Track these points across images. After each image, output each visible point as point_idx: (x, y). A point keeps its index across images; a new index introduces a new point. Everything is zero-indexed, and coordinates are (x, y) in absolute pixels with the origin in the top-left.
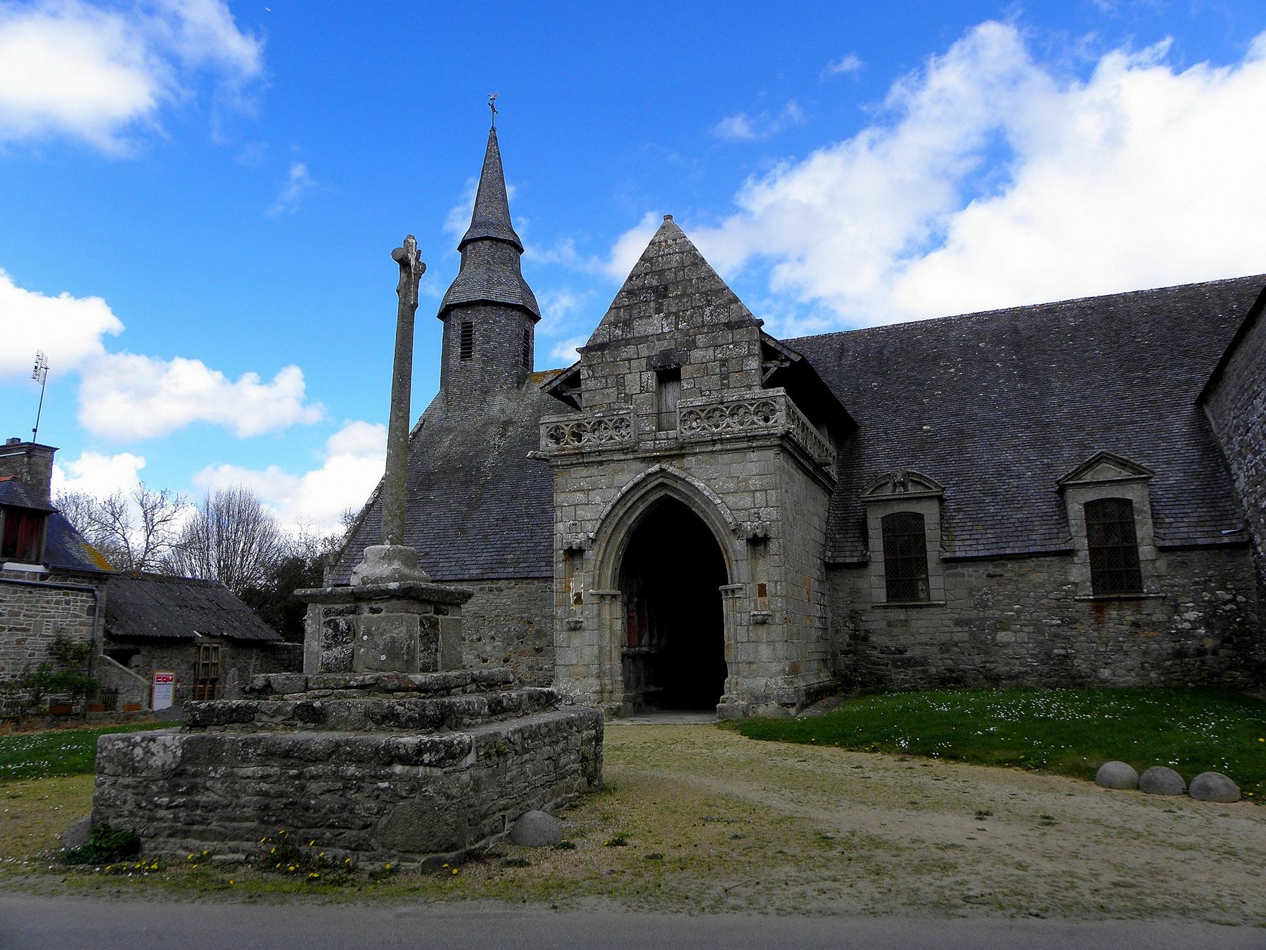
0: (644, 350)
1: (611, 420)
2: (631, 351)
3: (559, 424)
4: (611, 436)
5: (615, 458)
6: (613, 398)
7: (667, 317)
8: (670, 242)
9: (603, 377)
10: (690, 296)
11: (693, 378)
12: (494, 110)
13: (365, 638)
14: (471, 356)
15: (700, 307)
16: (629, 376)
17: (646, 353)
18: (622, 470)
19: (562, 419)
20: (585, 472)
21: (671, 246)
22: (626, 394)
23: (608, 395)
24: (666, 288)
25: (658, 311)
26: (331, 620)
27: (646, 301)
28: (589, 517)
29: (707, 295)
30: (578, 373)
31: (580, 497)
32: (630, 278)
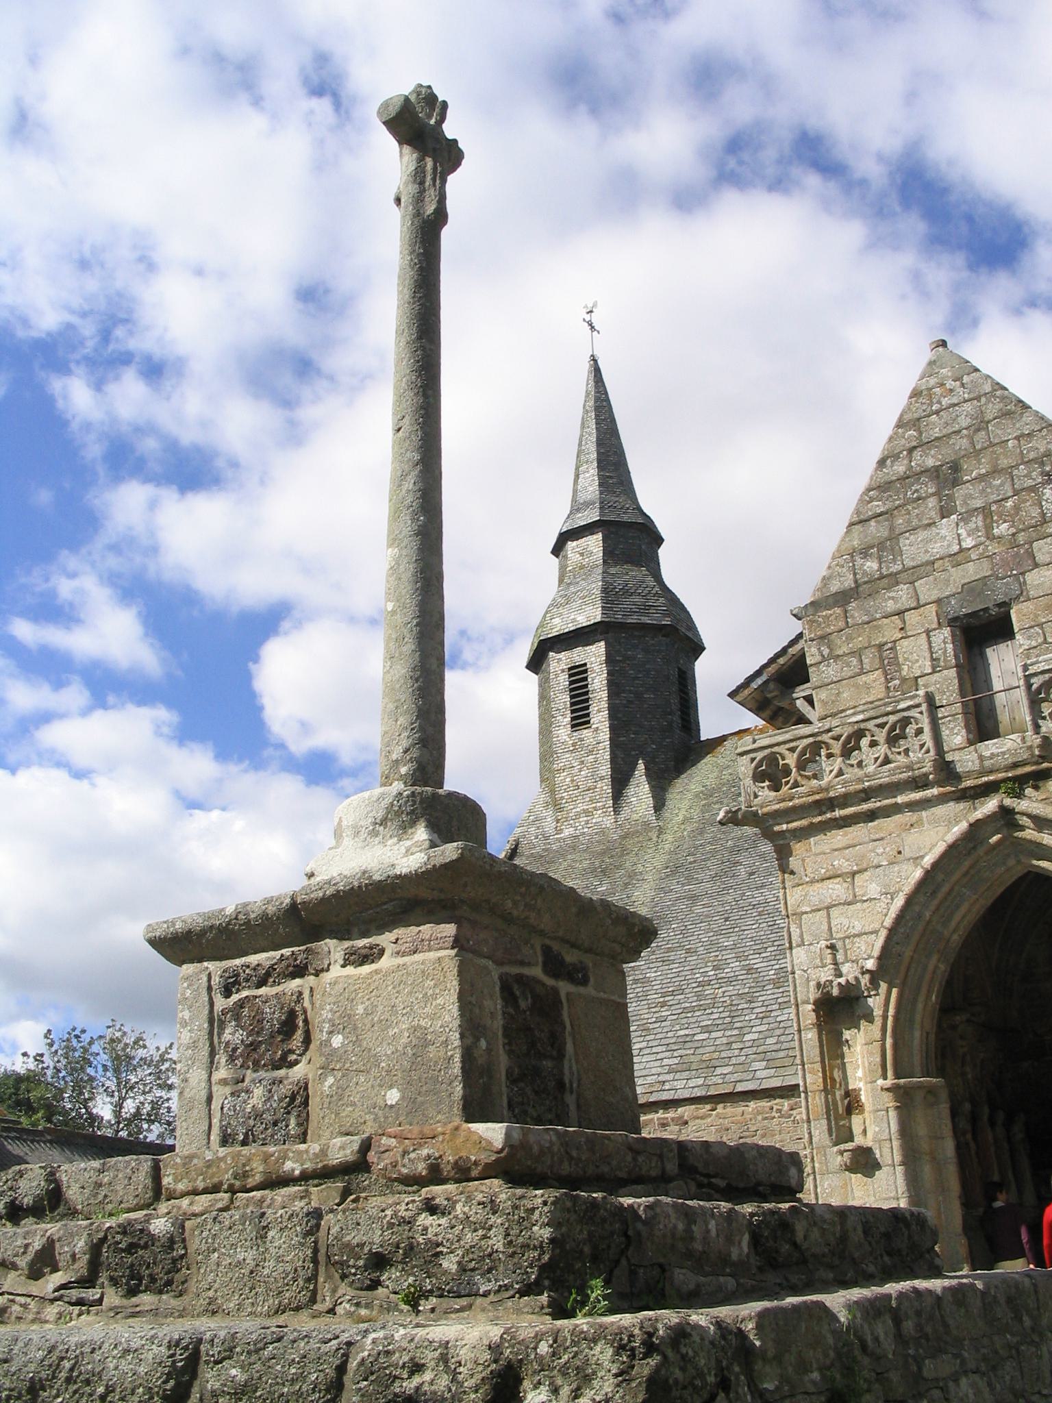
0: (927, 589)
1: (881, 726)
2: (902, 595)
3: (776, 749)
4: (886, 757)
5: (900, 799)
6: (878, 692)
7: (965, 518)
8: (950, 384)
9: (852, 653)
10: (1008, 472)
11: (1041, 625)
12: (592, 328)
13: (337, 1041)
14: (588, 722)
15: (1033, 489)
16: (905, 643)
17: (935, 594)
18: (920, 822)
19: (780, 739)
20: (838, 837)
21: (951, 390)
22: (904, 680)
23: (868, 687)
24: (955, 467)
25: (944, 513)
26: (241, 1004)
27: (919, 499)
28: (858, 928)
29: (1042, 464)
30: (802, 656)
31: (836, 890)
32: (882, 463)
